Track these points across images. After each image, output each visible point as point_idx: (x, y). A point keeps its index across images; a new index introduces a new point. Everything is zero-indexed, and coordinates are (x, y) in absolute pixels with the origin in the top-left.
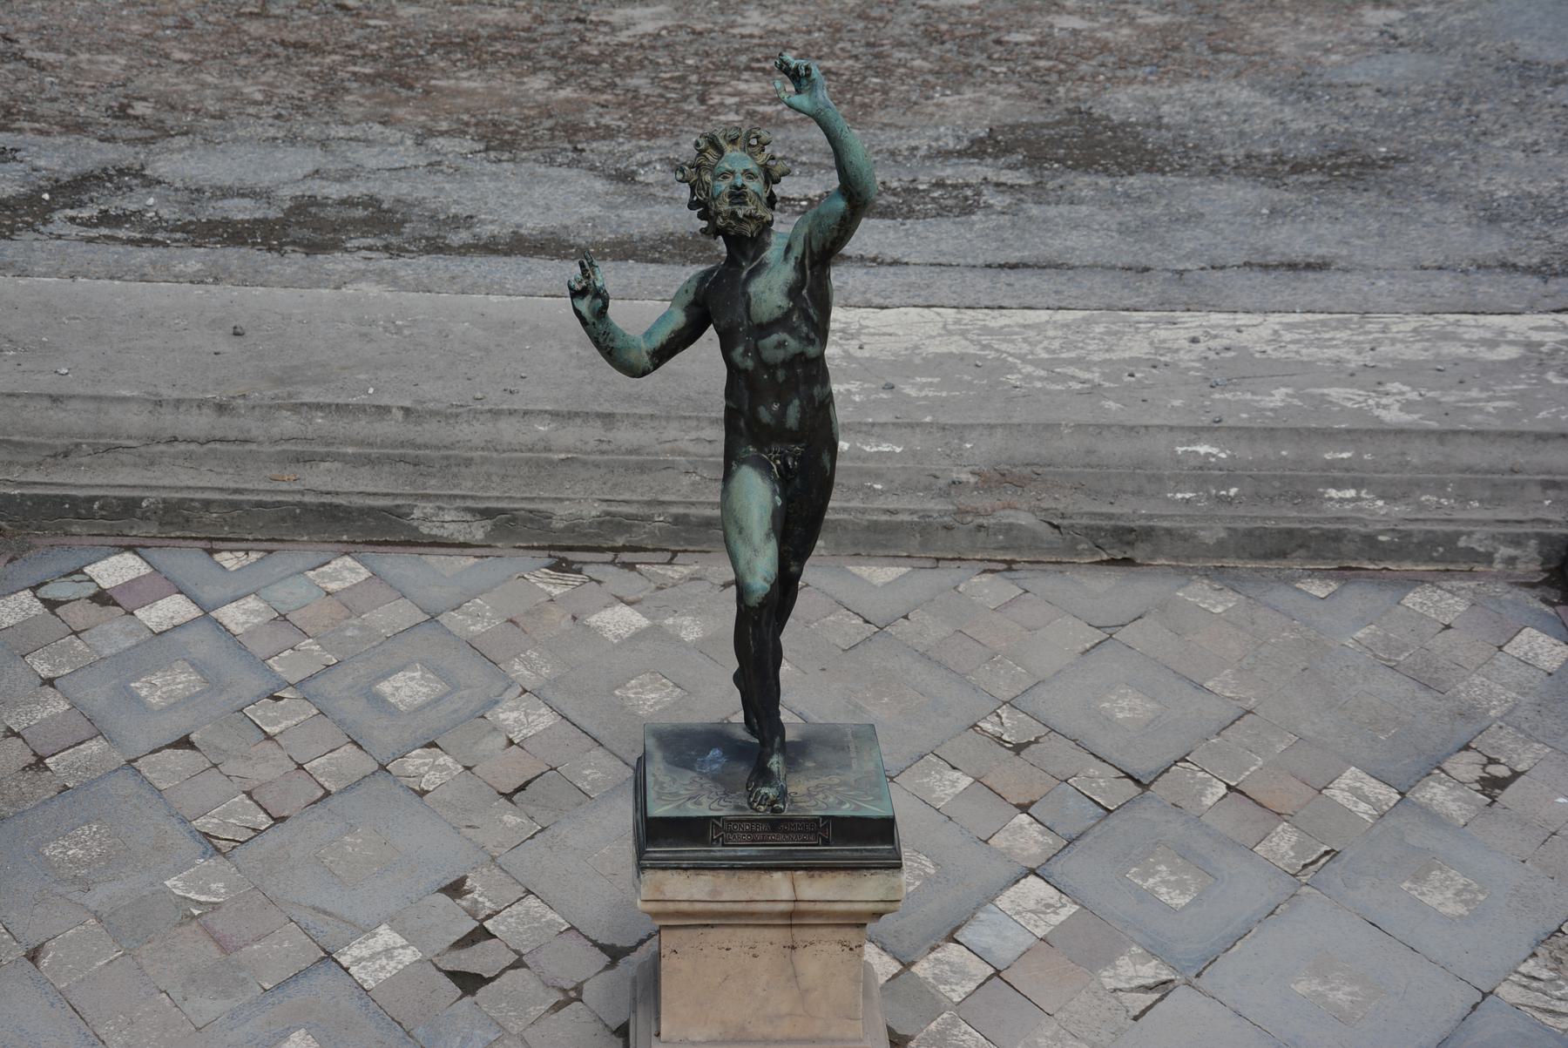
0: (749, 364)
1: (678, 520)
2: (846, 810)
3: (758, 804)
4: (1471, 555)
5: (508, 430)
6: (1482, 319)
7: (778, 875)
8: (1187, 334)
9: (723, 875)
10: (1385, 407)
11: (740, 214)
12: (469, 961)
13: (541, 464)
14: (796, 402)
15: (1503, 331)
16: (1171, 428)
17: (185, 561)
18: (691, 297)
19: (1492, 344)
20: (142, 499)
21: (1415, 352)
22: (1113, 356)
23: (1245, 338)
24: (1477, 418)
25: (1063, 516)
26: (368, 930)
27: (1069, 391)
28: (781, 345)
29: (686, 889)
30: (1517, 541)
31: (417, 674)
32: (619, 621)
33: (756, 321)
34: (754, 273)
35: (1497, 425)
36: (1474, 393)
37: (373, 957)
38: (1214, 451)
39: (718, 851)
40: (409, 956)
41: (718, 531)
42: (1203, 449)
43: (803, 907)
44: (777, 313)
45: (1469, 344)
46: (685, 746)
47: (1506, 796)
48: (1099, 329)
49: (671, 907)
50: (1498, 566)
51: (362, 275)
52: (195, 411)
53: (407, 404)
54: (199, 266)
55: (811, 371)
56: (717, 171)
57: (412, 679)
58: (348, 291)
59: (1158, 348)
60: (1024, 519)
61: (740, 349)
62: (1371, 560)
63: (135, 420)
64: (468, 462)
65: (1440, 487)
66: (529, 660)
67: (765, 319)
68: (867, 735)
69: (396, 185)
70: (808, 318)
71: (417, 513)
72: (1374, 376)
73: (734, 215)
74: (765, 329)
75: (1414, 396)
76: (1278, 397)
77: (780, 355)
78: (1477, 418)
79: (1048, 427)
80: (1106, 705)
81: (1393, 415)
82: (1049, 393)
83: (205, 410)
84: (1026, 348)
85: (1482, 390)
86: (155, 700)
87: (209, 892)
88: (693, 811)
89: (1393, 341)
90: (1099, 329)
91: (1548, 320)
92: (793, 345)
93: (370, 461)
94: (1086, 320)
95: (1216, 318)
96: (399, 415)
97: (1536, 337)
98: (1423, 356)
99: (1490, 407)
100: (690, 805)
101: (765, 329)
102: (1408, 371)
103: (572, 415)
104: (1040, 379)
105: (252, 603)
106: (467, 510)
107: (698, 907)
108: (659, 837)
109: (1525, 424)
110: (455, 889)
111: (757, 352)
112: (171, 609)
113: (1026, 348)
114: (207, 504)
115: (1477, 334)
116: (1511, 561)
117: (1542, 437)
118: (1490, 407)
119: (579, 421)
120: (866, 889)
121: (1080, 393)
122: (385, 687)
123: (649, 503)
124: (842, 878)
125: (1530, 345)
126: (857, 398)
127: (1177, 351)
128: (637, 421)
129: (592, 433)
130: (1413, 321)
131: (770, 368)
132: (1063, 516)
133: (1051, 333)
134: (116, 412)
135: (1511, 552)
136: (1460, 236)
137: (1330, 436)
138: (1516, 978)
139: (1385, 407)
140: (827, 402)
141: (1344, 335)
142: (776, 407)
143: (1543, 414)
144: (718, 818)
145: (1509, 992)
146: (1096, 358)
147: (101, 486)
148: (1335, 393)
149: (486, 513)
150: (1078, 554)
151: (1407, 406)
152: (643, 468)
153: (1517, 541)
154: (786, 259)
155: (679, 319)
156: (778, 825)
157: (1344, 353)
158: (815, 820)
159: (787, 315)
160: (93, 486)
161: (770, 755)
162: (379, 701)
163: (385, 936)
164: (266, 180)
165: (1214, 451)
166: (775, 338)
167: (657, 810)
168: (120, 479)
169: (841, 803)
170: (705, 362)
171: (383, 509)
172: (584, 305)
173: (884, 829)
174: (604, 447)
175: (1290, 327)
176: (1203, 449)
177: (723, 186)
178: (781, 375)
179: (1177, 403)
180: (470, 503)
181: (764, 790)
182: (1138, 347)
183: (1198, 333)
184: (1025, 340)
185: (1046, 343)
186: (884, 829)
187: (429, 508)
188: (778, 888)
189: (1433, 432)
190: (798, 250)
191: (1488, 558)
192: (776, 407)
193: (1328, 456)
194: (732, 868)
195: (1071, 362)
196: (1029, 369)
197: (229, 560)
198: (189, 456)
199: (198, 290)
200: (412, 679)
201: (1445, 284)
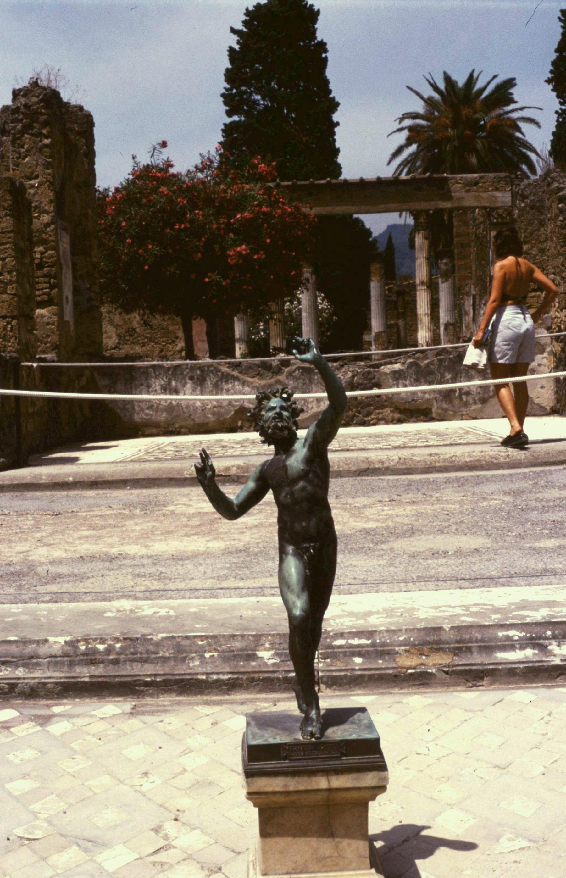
0: (289, 500)
2: (354, 737)
14: (314, 520)
39: (286, 763)
56: (267, 408)
70: (318, 476)
73: (276, 426)
74: (295, 481)
88: (272, 741)
101: (295, 481)
110: (157, 830)
120: (369, 779)
124: (355, 775)
144: (285, 744)
154: (304, 446)
170: (266, 512)
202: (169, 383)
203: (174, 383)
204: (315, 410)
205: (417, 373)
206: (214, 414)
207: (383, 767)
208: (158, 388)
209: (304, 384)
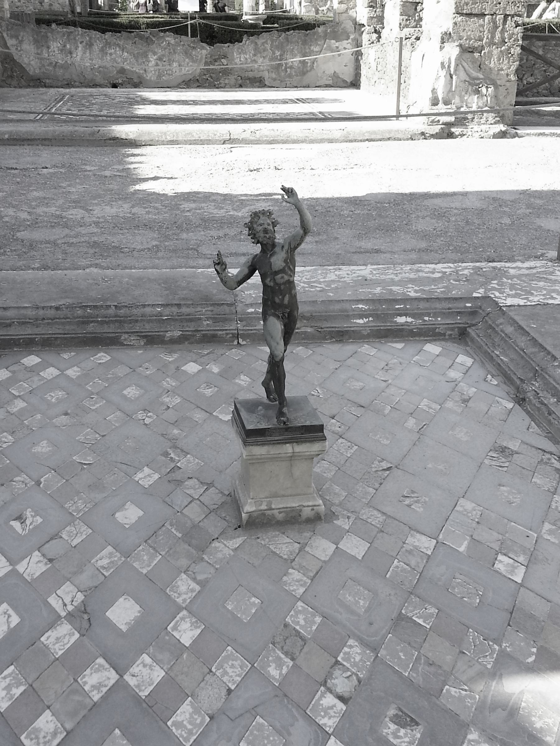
1: (204, 335)
2: (308, 423)
3: (279, 423)
4: (440, 334)
5: (148, 310)
6: (428, 265)
7: (287, 445)
8: (348, 273)
9: (271, 446)
10: (410, 292)
11: (268, 236)
12: (173, 476)
13: (159, 320)
14: (287, 295)
15: (434, 269)
16: (350, 301)
17: (51, 357)
18: (250, 264)
19: (433, 273)
20: (36, 338)
21: (412, 276)
22: (327, 280)
23: (363, 273)
24: (436, 294)
25: (321, 328)
26: (140, 469)
27: (316, 290)
28: (282, 277)
29: (259, 451)
30: (452, 329)
31: (134, 388)
32: (192, 368)
33: (274, 271)
34: (271, 255)
35: (442, 296)
36: (433, 287)
37: (145, 477)
38: (364, 307)
39: (269, 438)
40: (156, 476)
41: (264, 338)
42: (360, 306)
43: (296, 454)
44: (281, 268)
45: (426, 273)
46: (253, 406)
47: (470, 404)
48: (320, 272)
49: (255, 457)
50: (447, 337)
51: (91, 266)
52: (49, 310)
53: (116, 304)
54: (39, 265)
55: (291, 284)
56: (258, 223)
57: (133, 389)
58: (88, 270)
59: (339, 276)
60: (309, 330)
61: (269, 279)
62: (412, 337)
63: (31, 313)
64: (137, 321)
65: (429, 315)
66: (168, 381)
67: (277, 270)
68: (305, 399)
69: (92, 238)
71: (122, 338)
72: (402, 283)
73: (265, 237)
74: (276, 273)
75: (417, 288)
76: (378, 290)
77: (282, 281)
78: (436, 294)
79: (313, 302)
80: (348, 385)
81: (412, 294)
82: (311, 291)
83: (52, 309)
84: (300, 279)
85: (434, 286)
86: (53, 400)
87: (88, 460)
89: (405, 273)
90: (320, 272)
91: (445, 265)
92: (286, 278)
93: (107, 323)
94: (315, 270)
95: (352, 267)
96: (114, 308)
97: (444, 270)
98: (415, 277)
99: (438, 291)
100: (258, 424)
101: (276, 273)
102: (412, 281)
103: (168, 305)
104: (307, 287)
105: (75, 368)
106: (138, 336)
107: (263, 456)
108: (250, 436)
109: (450, 295)
111: (275, 280)
112: (51, 372)
113: (300, 279)
114: (56, 338)
115: (427, 270)
116: (451, 335)
117: (456, 299)
118: (438, 291)
119: (170, 307)
120: (315, 447)
121: (320, 291)
122: (125, 392)
123: (195, 331)
124: (308, 444)
125: (442, 272)
126: (254, 296)
127: (344, 277)
128: (188, 306)
129: (175, 310)
130: (409, 267)
131: (279, 285)
132: (321, 328)
133: (306, 274)
134: (23, 312)
135: (450, 332)
136: (414, 243)
137: (397, 301)
138: (488, 457)
139: (410, 292)
140: (295, 296)
141: (391, 271)
142: (280, 297)
143: (454, 292)
145: (486, 461)
146: (322, 280)
147: (22, 335)
148: (394, 288)
149: (145, 337)
150: (327, 340)
151: (416, 291)
152: (191, 320)
153: (452, 329)
155: (246, 271)
156: (288, 429)
157: (392, 276)
158: (299, 427)
159: (284, 268)
160: (20, 335)
161: (283, 407)
162: (125, 396)
163: (147, 470)
164: (52, 238)
165: (364, 307)
166: (280, 275)
167: (249, 427)
168: (28, 331)
169: (306, 421)
171: (112, 337)
172: (218, 267)
173: (321, 428)
174: (179, 314)
175: (375, 269)
176: (360, 306)
177: (260, 228)
178: (282, 287)
179: (350, 293)
180: (139, 334)
181: (282, 419)
182: (332, 277)
183: (349, 273)
184: (299, 276)
185: (305, 277)
186: (321, 428)
187: (126, 336)
188: (289, 448)
189: (425, 298)
190: (286, 247)
191: (444, 335)
192: (280, 297)
193: (397, 307)
194: (274, 444)
195: (314, 282)
196: (302, 284)
197: (66, 356)
198: (48, 324)
199: (40, 273)
200: (133, 389)
201: (414, 256)
202: (65, 46)
203: (68, 46)
204: (178, 74)
205: (255, 49)
206: (99, 72)
207: (324, 439)
208: (56, 49)
209: (170, 53)
